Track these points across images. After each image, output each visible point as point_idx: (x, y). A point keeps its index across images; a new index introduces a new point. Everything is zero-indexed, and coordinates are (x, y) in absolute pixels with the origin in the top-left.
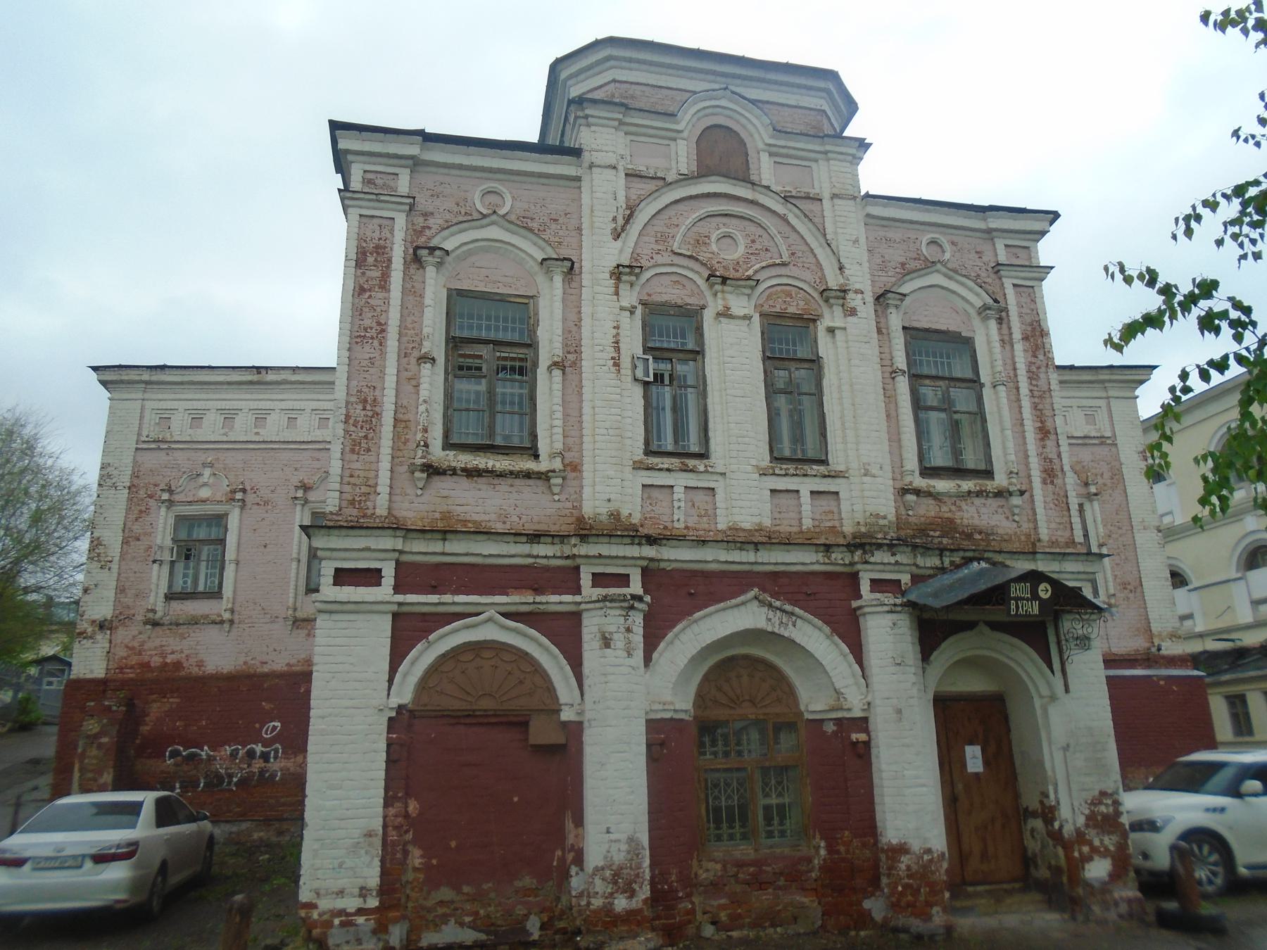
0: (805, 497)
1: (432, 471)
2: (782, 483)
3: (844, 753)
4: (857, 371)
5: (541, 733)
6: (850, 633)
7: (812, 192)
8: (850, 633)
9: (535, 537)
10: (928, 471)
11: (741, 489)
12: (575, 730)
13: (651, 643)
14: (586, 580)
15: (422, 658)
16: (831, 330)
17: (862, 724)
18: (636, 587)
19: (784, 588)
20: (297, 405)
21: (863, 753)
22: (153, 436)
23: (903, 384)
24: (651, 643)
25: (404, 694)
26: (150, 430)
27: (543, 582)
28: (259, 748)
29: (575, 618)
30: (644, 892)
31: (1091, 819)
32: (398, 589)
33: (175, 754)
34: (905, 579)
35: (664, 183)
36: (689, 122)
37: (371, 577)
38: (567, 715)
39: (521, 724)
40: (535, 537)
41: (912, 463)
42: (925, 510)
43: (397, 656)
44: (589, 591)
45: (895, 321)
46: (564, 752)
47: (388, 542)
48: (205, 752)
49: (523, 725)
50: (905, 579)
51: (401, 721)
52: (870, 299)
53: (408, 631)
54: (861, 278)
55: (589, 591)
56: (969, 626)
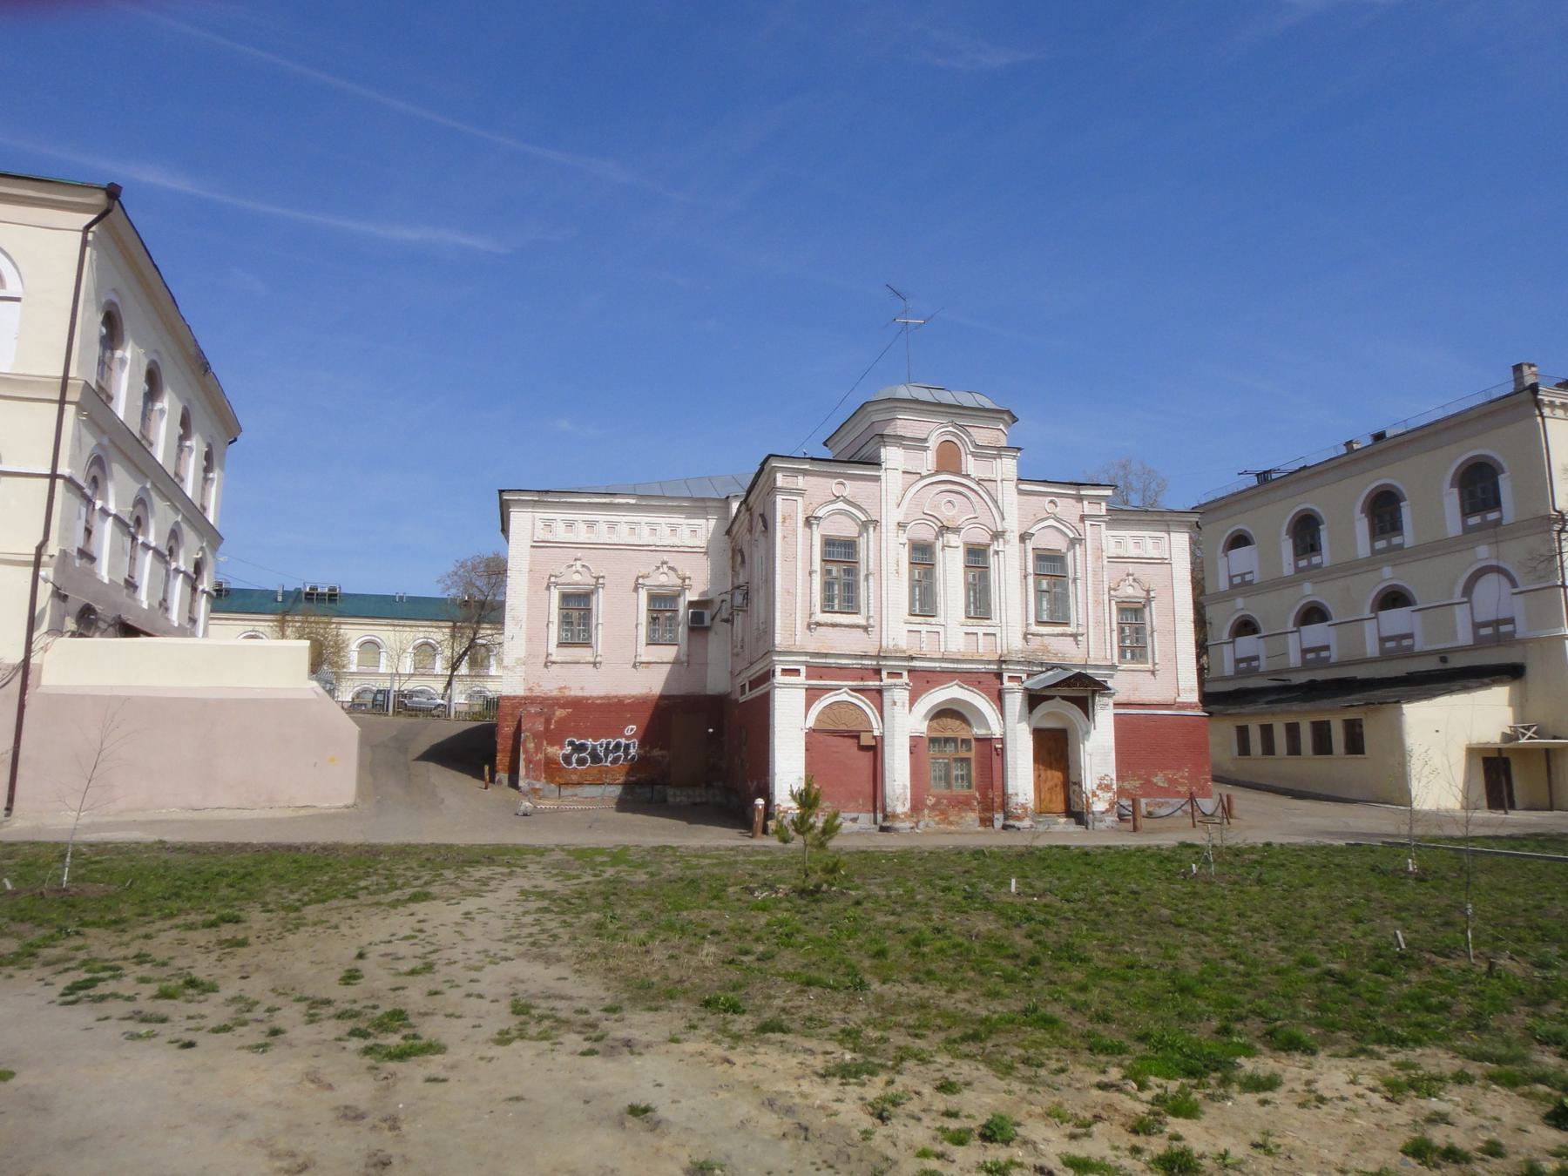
0: (981, 636)
1: (819, 624)
2: (970, 630)
3: (992, 752)
4: (1010, 574)
5: (866, 740)
6: (999, 698)
7: (993, 477)
8: (999, 698)
9: (862, 657)
10: (1040, 623)
11: (952, 633)
12: (880, 740)
13: (912, 704)
14: (884, 674)
15: (818, 707)
16: (997, 552)
17: (1002, 740)
18: (905, 678)
19: (970, 679)
20: (635, 519)
21: (1002, 753)
22: (542, 538)
23: (1031, 579)
24: (912, 704)
25: (811, 723)
26: (541, 534)
27: (871, 674)
28: (623, 741)
29: (880, 691)
30: (908, 805)
31: (1099, 786)
32: (808, 677)
33: (571, 743)
34: (1024, 677)
35: (923, 478)
36: (933, 443)
37: (797, 672)
38: (876, 733)
39: (856, 736)
40: (862, 657)
41: (1032, 620)
42: (1035, 643)
43: (808, 706)
44: (886, 681)
45: (1030, 545)
46: (875, 750)
47: (803, 659)
48: (590, 742)
49: (858, 737)
50: (1024, 677)
51: (811, 734)
52: (1017, 535)
53: (813, 694)
54: (1013, 526)
55: (886, 681)
56: (1052, 697)
